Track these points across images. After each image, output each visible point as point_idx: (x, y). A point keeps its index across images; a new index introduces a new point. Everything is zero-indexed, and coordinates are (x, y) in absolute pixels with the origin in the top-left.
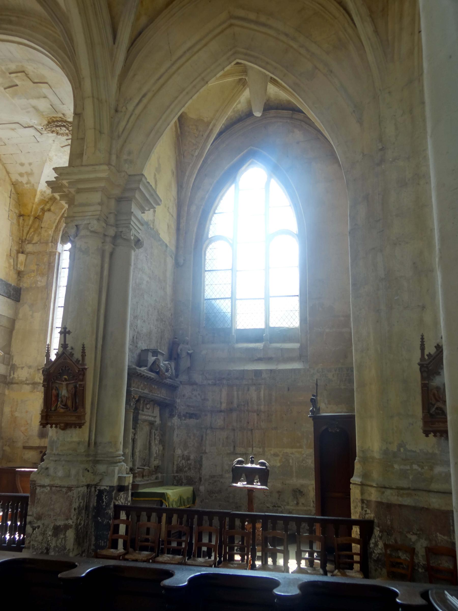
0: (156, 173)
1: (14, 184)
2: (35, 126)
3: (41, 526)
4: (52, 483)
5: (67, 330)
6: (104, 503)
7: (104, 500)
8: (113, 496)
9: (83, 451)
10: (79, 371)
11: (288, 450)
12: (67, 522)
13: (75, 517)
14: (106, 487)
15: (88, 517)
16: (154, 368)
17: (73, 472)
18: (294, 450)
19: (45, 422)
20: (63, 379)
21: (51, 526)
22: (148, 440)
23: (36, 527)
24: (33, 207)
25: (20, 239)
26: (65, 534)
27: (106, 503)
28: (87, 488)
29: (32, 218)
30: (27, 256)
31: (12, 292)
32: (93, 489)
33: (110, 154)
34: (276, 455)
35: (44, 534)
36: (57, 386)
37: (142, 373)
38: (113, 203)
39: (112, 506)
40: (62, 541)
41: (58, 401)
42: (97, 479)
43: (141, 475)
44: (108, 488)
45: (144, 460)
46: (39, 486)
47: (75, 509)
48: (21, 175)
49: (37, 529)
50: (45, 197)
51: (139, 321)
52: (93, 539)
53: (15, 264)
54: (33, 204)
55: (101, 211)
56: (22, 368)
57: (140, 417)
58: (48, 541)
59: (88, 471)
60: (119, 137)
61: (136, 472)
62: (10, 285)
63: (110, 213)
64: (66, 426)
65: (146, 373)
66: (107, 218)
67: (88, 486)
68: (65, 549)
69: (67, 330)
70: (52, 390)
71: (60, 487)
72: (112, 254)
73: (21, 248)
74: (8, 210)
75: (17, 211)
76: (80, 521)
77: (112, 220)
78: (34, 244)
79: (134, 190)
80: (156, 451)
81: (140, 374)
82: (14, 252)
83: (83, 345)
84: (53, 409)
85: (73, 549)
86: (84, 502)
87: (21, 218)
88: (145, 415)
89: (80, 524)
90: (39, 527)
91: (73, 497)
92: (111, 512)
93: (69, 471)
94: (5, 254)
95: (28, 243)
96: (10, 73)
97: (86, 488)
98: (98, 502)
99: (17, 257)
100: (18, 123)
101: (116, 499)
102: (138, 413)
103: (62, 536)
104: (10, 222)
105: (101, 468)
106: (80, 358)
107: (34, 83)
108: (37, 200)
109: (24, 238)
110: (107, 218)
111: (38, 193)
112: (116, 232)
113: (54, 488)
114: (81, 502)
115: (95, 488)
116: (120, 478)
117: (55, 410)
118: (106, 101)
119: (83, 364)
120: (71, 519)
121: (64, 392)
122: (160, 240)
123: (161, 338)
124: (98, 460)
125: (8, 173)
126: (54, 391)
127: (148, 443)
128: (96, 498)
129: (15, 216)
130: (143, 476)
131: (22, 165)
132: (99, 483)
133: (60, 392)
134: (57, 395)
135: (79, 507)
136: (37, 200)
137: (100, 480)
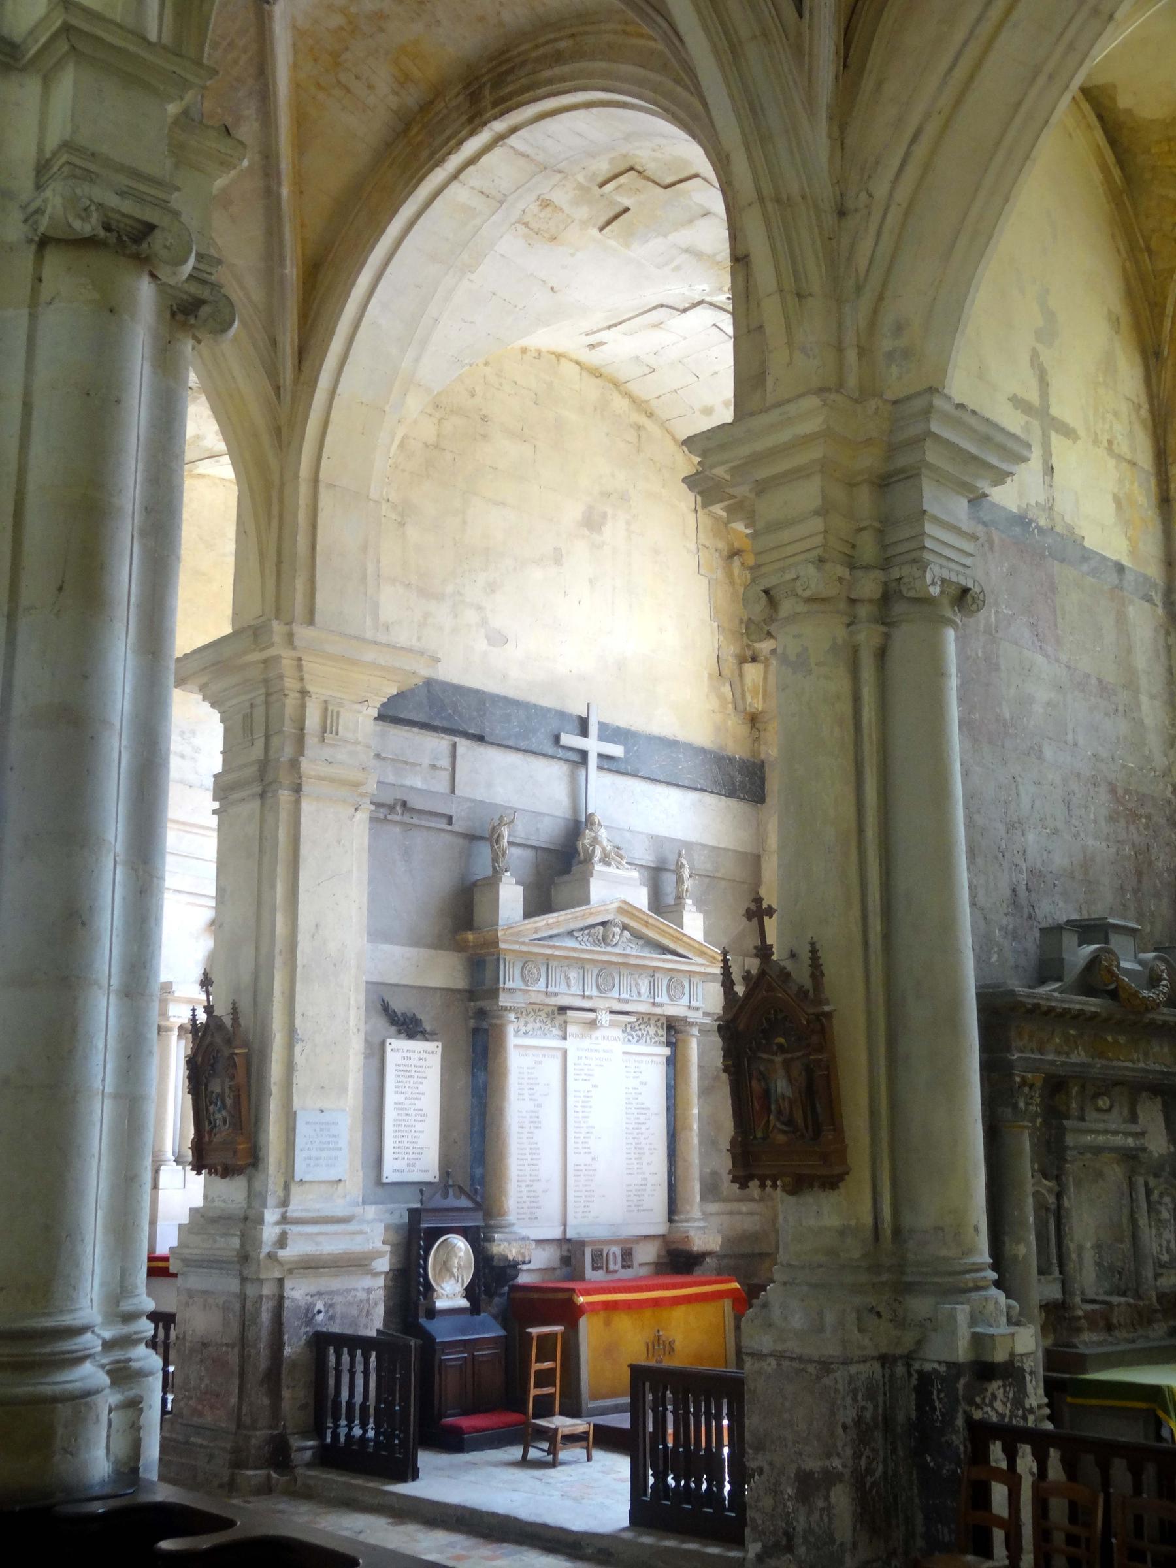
0: (1039, 347)
2: (707, 299)
3: (766, 1468)
4: (779, 1347)
5: (765, 906)
6: (938, 1413)
7: (937, 1403)
8: (961, 1392)
9: (856, 1254)
10: (808, 1021)
12: (827, 1463)
13: (849, 1452)
14: (936, 1366)
15: (894, 1451)
16: (1095, 979)
17: (830, 1318)
19: (741, 1173)
20: (775, 1048)
21: (792, 1471)
22: (1126, 1211)
26: (827, 1498)
27: (943, 1415)
28: (883, 1366)
31: (739, 778)
32: (900, 1370)
33: (840, 350)
35: (775, 1491)
36: (762, 1068)
37: (1043, 1002)
38: (864, 497)
39: (960, 1422)
40: (821, 1516)
41: (769, 1111)
42: (909, 1340)
43: (1102, 1324)
44: (943, 1369)
45: (1120, 1273)
46: (748, 1354)
47: (845, 1427)
49: (756, 1477)
51: (1031, 837)
52: (919, 1518)
53: (738, 695)
55: (826, 531)
57: (1070, 1140)
58: (788, 1514)
59: (879, 1315)
60: (859, 289)
61: (1080, 1313)
62: (731, 760)
63: (861, 529)
64: (799, 1185)
65: (1057, 1000)
66: (853, 546)
67: (884, 1359)
68: (833, 1541)
69: (765, 906)
70: (750, 1079)
71: (800, 1359)
72: (882, 654)
74: (693, 547)
76: (869, 1463)
77: (868, 550)
79: (917, 442)
80: (1169, 1242)
81: (1037, 1006)
82: (730, 662)
83: (813, 944)
84: (759, 1135)
85: (855, 1545)
86: (876, 1407)
88: (1091, 1131)
89: (869, 1471)
90: (761, 1471)
91: (836, 1391)
92: (958, 1440)
93: (821, 1313)
94: (706, 674)
96: (601, 185)
97: (877, 1366)
98: (920, 1408)
99: (741, 675)
100: (662, 306)
101: (971, 1402)
102: (1062, 1131)
103: (821, 1503)
104: (706, 581)
105: (920, 1306)
106: (808, 983)
107: (666, 187)
110: (853, 546)
112: (885, 584)
113: (786, 1363)
114: (864, 1408)
115: (908, 1365)
116: (978, 1340)
117: (764, 1139)
118: (804, 197)
119: (819, 1001)
120: (838, 1455)
121: (781, 1086)
122: (1086, 556)
123: (1139, 874)
124: (911, 1284)
126: (754, 1083)
127: (1125, 1221)
128: (914, 1396)
130: (1110, 1328)
132: (914, 1351)
133: (772, 1086)
134: (767, 1094)
135: (858, 1422)
137: (919, 1343)
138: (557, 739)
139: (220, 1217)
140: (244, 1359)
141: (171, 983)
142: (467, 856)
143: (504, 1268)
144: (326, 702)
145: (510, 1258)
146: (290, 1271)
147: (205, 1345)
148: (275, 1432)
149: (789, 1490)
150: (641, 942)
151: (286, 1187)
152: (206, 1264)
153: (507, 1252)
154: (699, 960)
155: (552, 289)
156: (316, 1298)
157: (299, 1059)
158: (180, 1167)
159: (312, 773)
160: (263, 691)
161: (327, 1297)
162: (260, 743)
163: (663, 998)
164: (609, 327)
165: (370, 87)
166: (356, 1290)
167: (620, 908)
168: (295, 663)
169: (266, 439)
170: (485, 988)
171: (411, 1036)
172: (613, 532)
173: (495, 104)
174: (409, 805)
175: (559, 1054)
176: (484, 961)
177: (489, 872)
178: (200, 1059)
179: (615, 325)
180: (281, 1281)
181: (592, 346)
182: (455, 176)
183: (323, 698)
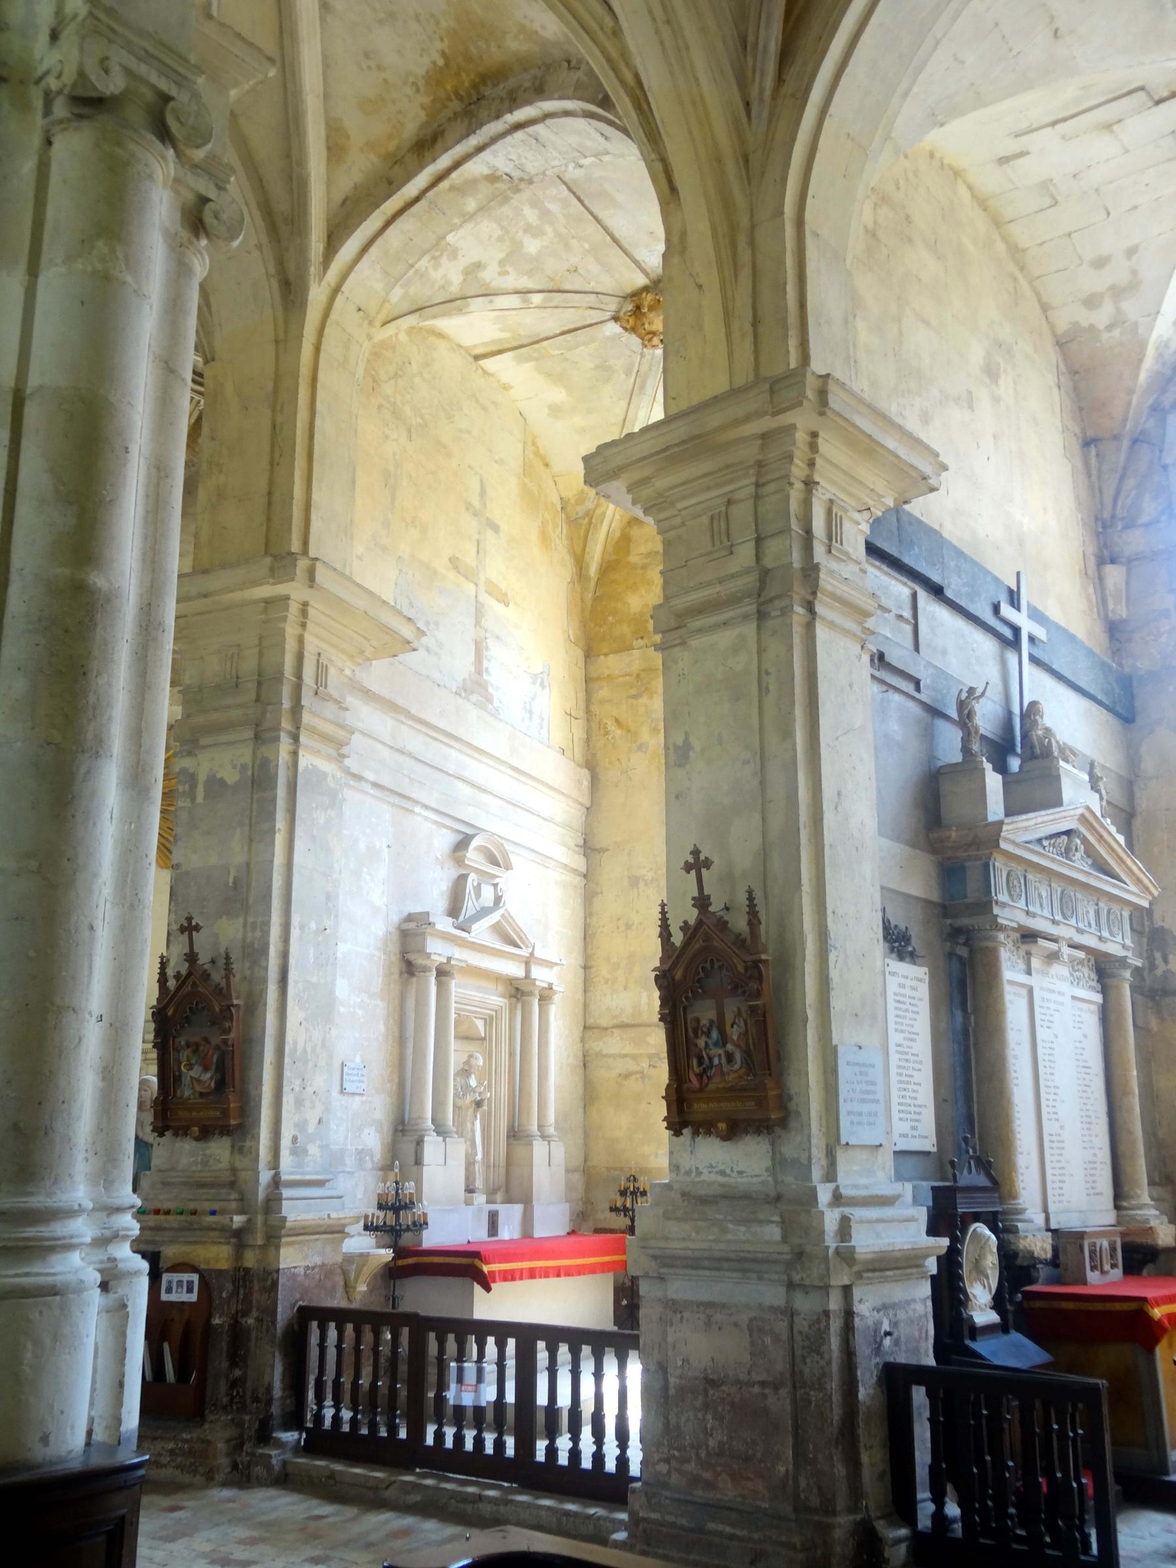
1: (1062, 344)
24: (1129, 404)
25: (1096, 519)
29: (1126, 443)
30: (1129, 571)
48: (1091, 302)
50: (1164, 364)
54: (1131, 392)
73: (1105, 546)
75: (1077, 430)
78: (1146, 525)
87: (1093, 450)
95: (1125, 528)
99: (1101, 578)
108: (1143, 376)
109: (1106, 515)
111: (1150, 352)
125: (1045, 308)
129: (1076, 447)
131: (1100, 263)
136: (1143, 376)
138: (996, 609)
139: (724, 1197)
140: (799, 1407)
141: (428, 913)
142: (928, 736)
143: (1028, 1267)
144: (831, 501)
145: (1036, 1254)
146: (859, 1275)
147: (712, 1383)
148: (859, 1517)
150: (1090, 861)
151: (831, 1154)
152: (706, 1263)
153: (1033, 1248)
154: (1133, 888)
155: (1056, 31)
156: (882, 1313)
157: (834, 974)
158: (441, 1139)
159: (829, 588)
160: (753, 479)
161: (891, 1313)
162: (745, 554)
163: (1105, 934)
164: (1054, 124)
166: (914, 1300)
167: (1082, 815)
168: (808, 439)
169: (731, 168)
170: (967, 901)
171: (901, 958)
172: (1005, 386)
174: (888, 658)
175: (1024, 992)
176: (963, 868)
177: (958, 758)
178: (679, 975)
179: (1064, 120)
180: (847, 1290)
181: (1003, 161)
183: (828, 496)
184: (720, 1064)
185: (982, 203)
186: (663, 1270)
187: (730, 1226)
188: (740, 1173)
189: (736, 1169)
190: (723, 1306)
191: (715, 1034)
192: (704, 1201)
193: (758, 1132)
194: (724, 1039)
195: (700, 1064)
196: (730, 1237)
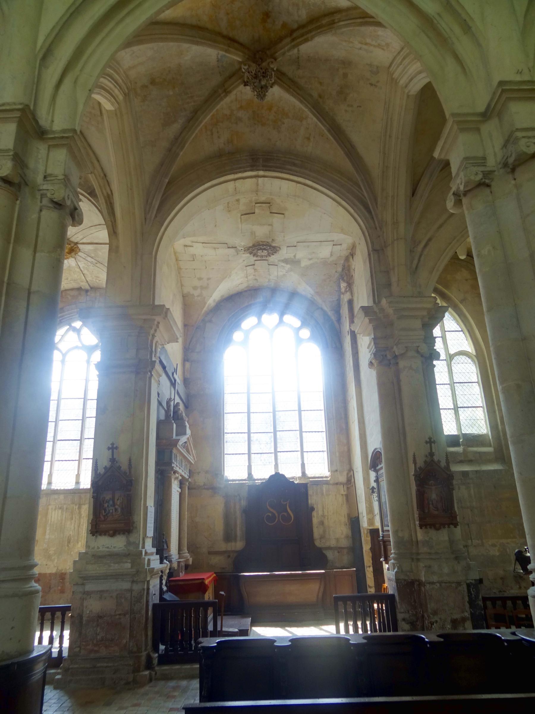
3: (439, 620)
11: (504, 541)
12: (463, 615)
14: (471, 581)
18: (509, 540)
23: (433, 623)
34: (494, 545)
44: (473, 582)
48: (195, 288)
49: (435, 624)
56: (199, 473)
71: (449, 582)
90: (437, 622)
92: (481, 603)
96: (256, 203)
108: (203, 311)
113: (443, 585)
121: (434, 496)
131: (200, 279)
136: (203, 311)
147: (100, 617)
149: (449, 626)
164: (203, 243)
165: (219, 137)
173: (263, 166)
178: (100, 484)
182: (235, 180)
184: (113, 512)
185: (175, 253)
186: (85, 581)
187: (112, 564)
188: (114, 547)
189: (113, 546)
190: (107, 591)
191: (111, 502)
192: (100, 557)
193: (124, 534)
194: (114, 505)
195: (105, 512)
196: (112, 568)
